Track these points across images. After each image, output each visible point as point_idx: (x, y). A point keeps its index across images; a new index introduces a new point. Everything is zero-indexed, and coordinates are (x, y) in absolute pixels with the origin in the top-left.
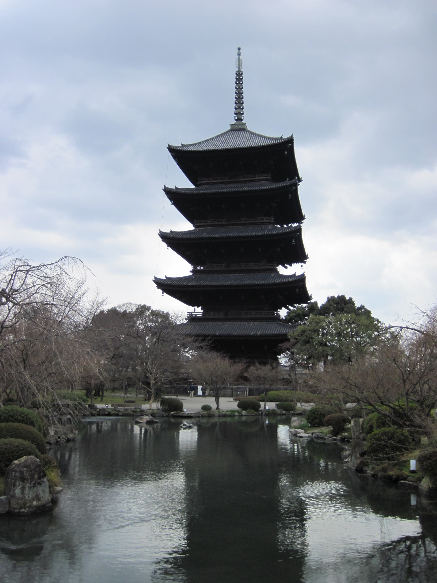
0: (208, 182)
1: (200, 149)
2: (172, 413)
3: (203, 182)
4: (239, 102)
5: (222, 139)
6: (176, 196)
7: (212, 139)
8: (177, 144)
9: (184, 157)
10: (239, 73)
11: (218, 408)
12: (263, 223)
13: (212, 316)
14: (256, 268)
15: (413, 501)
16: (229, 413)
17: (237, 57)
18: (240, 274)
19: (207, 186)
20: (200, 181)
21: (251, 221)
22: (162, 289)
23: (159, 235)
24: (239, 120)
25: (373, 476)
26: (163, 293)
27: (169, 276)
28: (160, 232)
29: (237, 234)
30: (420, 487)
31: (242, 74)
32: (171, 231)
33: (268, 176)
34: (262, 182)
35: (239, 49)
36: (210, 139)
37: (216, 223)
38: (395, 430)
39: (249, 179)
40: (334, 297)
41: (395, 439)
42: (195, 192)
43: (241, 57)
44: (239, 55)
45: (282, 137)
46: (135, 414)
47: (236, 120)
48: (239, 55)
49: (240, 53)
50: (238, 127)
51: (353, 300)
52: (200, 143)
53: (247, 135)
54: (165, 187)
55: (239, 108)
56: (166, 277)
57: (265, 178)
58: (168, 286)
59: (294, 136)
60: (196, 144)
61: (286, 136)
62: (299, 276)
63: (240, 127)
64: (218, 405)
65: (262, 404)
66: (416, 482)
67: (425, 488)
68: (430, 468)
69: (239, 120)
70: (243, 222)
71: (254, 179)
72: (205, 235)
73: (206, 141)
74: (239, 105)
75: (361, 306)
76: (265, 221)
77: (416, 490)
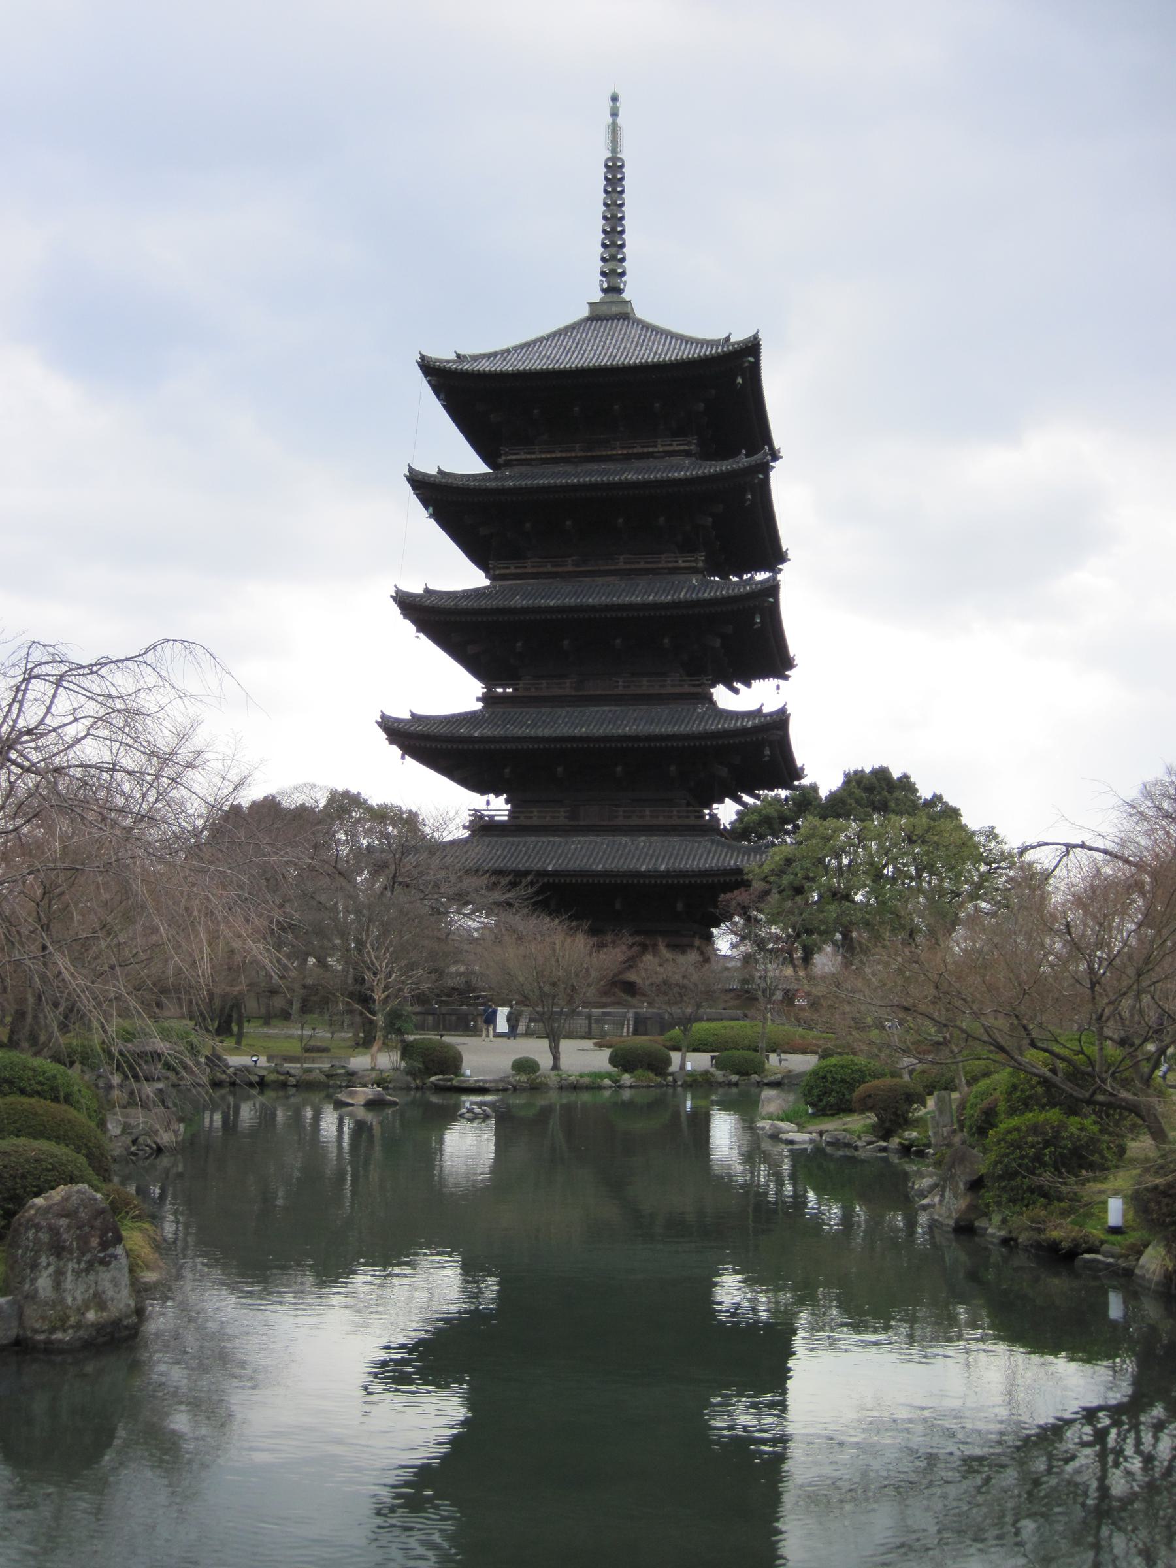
0: (528, 456)
1: (507, 367)
2: (433, 1079)
3: (514, 457)
4: (613, 244)
5: (567, 342)
6: (439, 496)
7: (540, 340)
8: (443, 352)
9: (464, 391)
10: (614, 164)
11: (556, 1067)
12: (674, 571)
13: (535, 821)
14: (655, 690)
15: (1116, 1308)
16: (586, 1080)
17: (610, 120)
18: (613, 708)
19: (523, 469)
20: (506, 454)
21: (642, 565)
22: (400, 747)
23: (394, 599)
24: (613, 290)
25: (1005, 1242)
26: (403, 758)
27: (422, 711)
28: (398, 591)
29: (604, 600)
30: (1137, 1271)
31: (622, 166)
32: (427, 590)
33: (688, 444)
34: (675, 460)
35: (615, 99)
36: (534, 342)
37: (549, 568)
38: (1063, 1117)
40: (863, 771)
41: (1064, 1142)
42: (493, 485)
43: (620, 120)
44: (614, 114)
45: (727, 339)
46: (331, 1082)
47: (604, 291)
48: (614, 114)
49: (618, 109)
50: (611, 310)
51: (912, 780)
52: (508, 351)
53: (635, 332)
54: (411, 469)
55: (613, 258)
56: (413, 715)
57: (682, 448)
58: (418, 739)
59: (760, 335)
60: (495, 354)
61: (740, 335)
62: (771, 714)
63: (614, 309)
64: (556, 1058)
65: (675, 1057)
66: (1126, 1256)
67: (1154, 1273)
68: (1168, 1220)
69: (613, 290)
70: (622, 566)
71: (651, 450)
72: (518, 601)
73: (522, 346)
74: (613, 250)
75: (935, 796)
76: (681, 564)
77: (1126, 1278)
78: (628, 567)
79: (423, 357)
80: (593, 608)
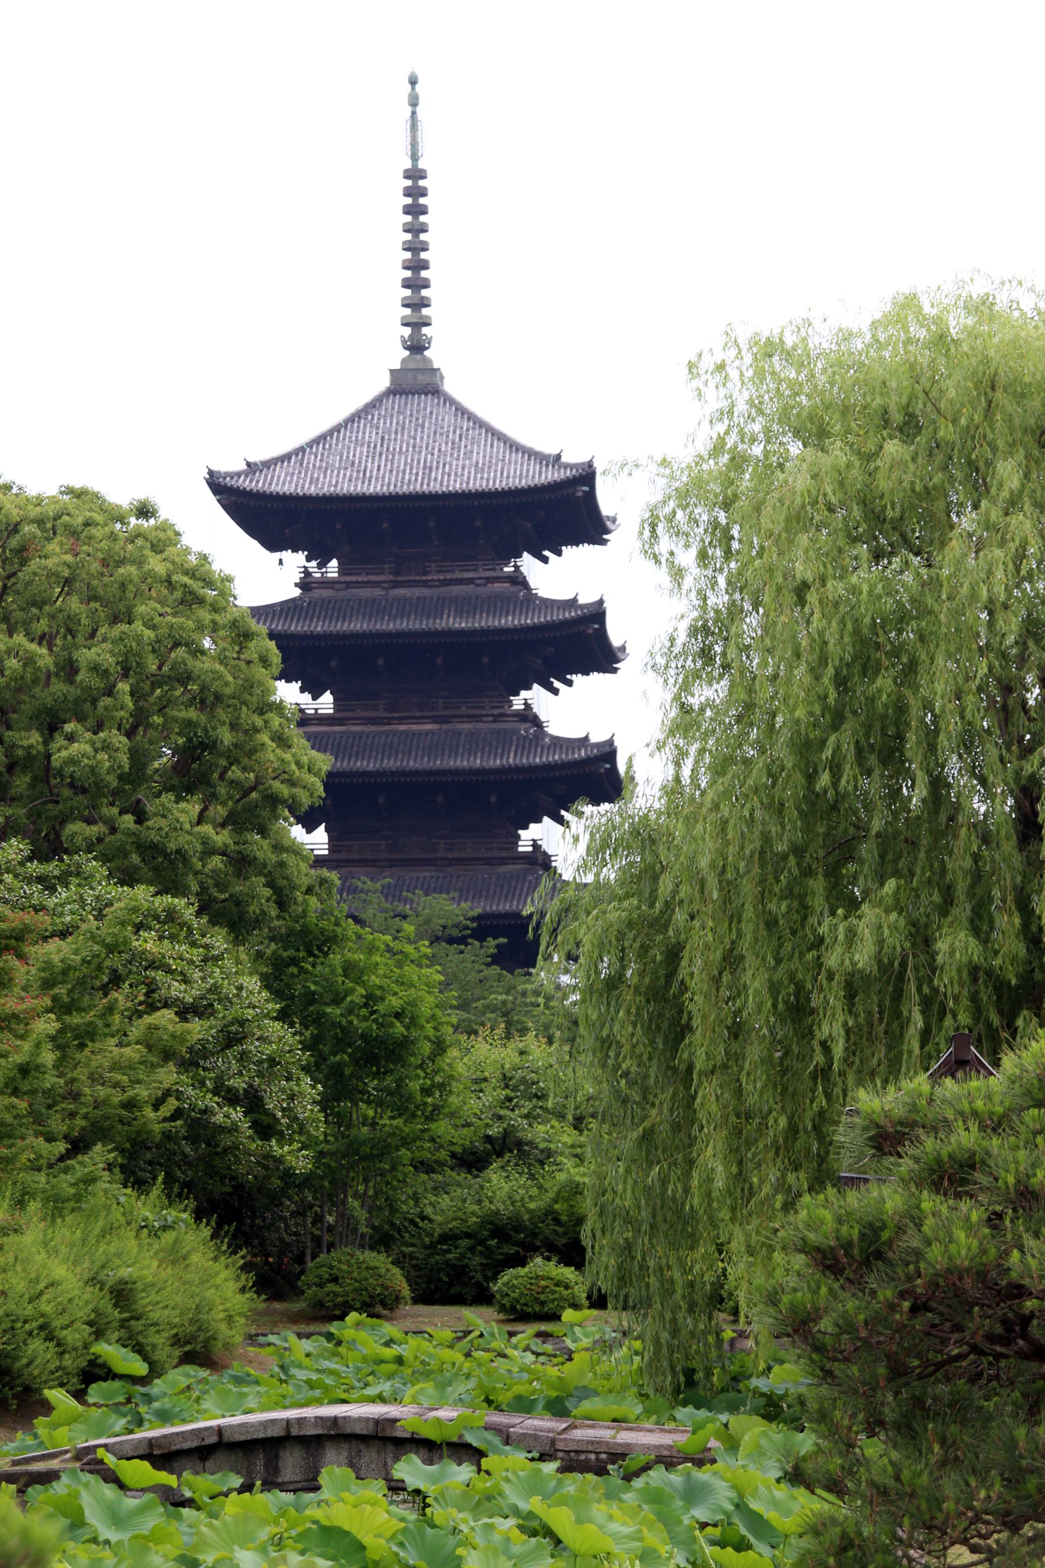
5: (370, 435)
7: (337, 429)
8: (230, 463)
21: (463, 710)
24: (416, 346)
35: (413, 82)
36: (330, 433)
37: (359, 713)
39: (458, 575)
44: (414, 102)
45: (558, 457)
48: (414, 102)
50: (416, 382)
52: (301, 450)
53: (448, 418)
69: (416, 346)
71: (471, 575)
78: (448, 712)
79: (211, 473)
80: (417, 773)
